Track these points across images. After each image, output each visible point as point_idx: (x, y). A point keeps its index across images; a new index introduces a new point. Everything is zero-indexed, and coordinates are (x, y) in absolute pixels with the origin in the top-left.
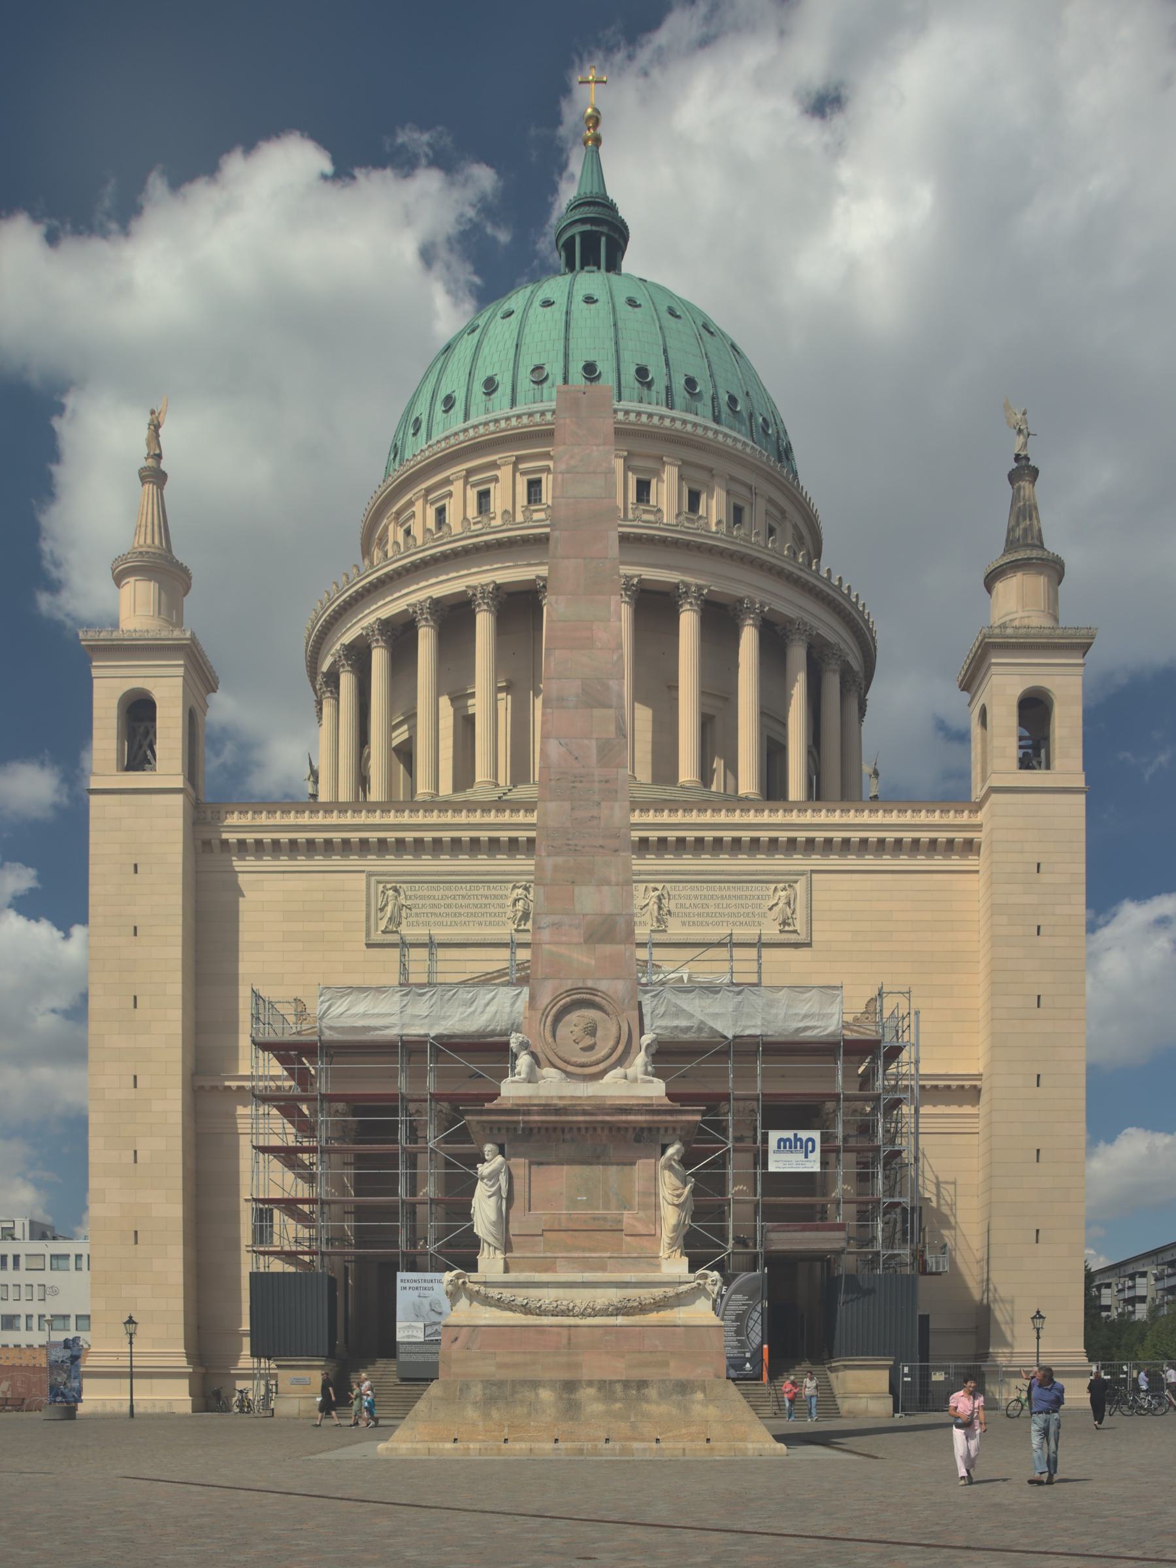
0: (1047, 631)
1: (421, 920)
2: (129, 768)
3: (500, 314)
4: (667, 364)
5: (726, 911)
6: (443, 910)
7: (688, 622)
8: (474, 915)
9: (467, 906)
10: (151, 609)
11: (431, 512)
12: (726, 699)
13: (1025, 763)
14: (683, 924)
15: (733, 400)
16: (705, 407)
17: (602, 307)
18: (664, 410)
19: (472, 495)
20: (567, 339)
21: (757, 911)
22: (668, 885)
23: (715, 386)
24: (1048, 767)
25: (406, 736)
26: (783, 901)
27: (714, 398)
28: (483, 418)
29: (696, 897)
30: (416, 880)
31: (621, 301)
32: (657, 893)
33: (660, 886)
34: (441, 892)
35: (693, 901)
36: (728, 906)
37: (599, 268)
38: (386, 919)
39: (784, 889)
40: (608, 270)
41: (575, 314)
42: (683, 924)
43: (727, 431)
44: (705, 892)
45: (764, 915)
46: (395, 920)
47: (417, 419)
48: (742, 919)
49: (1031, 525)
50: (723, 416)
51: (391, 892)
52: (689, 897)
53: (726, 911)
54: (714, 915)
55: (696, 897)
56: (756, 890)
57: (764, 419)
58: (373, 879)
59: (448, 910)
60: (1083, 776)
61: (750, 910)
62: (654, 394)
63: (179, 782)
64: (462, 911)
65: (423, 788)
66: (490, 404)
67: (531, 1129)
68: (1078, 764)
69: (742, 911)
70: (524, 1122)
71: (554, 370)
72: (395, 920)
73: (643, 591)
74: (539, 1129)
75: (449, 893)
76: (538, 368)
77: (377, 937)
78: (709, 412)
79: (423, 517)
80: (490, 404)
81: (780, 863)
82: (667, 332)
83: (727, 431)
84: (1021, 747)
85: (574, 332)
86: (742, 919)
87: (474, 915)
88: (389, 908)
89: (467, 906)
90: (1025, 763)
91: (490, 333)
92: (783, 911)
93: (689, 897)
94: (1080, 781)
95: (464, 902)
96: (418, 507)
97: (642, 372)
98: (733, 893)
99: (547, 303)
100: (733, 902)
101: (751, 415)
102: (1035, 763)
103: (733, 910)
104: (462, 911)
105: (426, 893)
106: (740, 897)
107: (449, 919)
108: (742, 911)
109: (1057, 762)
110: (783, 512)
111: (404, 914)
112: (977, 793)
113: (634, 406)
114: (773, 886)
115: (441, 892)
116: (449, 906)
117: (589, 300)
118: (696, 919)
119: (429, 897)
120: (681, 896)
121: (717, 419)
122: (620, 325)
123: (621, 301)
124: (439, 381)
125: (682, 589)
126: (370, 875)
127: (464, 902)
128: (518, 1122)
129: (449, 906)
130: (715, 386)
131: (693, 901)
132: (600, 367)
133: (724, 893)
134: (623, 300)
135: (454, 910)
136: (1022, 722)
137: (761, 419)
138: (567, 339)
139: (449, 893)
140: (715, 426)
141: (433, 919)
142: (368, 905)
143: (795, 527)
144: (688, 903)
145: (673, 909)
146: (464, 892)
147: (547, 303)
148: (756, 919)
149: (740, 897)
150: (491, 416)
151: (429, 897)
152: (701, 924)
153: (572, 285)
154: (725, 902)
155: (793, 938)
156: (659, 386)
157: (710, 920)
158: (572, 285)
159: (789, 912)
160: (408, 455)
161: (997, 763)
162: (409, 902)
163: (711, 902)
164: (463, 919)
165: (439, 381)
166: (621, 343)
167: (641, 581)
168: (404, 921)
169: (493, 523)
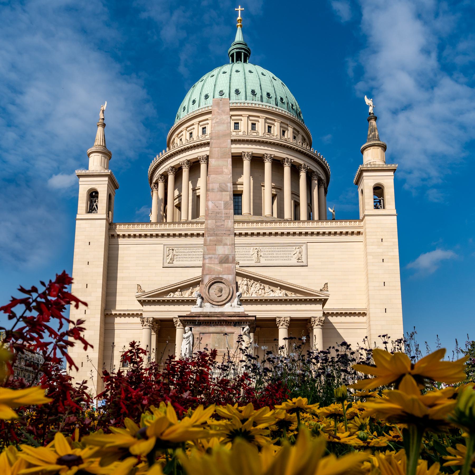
0: (381, 166)
1: (180, 259)
2: (89, 212)
3: (210, 76)
4: (261, 89)
5: (280, 256)
6: (187, 256)
7: (268, 165)
8: (198, 258)
9: (196, 255)
10: (99, 164)
11: (188, 134)
12: (280, 189)
13: (376, 207)
14: (266, 260)
15: (282, 99)
16: (273, 101)
17: (241, 73)
18: (260, 103)
19: (200, 129)
20: (230, 83)
21: (290, 255)
22: (261, 248)
23: (276, 95)
24: (384, 208)
25: (178, 202)
26: (298, 252)
27: (276, 99)
28: (204, 106)
29: (270, 251)
30: (179, 246)
31: (247, 72)
32: (257, 250)
33: (258, 248)
34: (187, 250)
35: (269, 253)
36: (280, 254)
37: (241, 61)
38: (169, 259)
39: (299, 248)
40: (244, 62)
41: (233, 76)
42: (266, 260)
43: (280, 108)
44: (273, 250)
45: (292, 257)
46: (172, 259)
47: (184, 107)
48: (285, 258)
49: (375, 134)
50: (279, 104)
51: (171, 251)
52: (267, 251)
53: (280, 256)
54: (276, 257)
55: (270, 251)
56: (289, 249)
57: (292, 105)
58: (165, 246)
59: (189, 256)
60: (395, 211)
61: (287, 255)
62: (257, 98)
63: (104, 216)
64: (194, 256)
65: (184, 218)
66: (206, 102)
67: (200, 322)
68: (394, 207)
69: (285, 255)
70: (199, 320)
71: (226, 92)
72: (172, 259)
73: (253, 157)
74: (203, 322)
75: (190, 251)
76: (221, 91)
77: (166, 265)
78: (274, 103)
79: (186, 135)
80: (206, 102)
81: (297, 239)
82: (261, 80)
83: (280, 108)
84: (374, 202)
85: (232, 81)
86: (285, 258)
87: (198, 258)
88: (170, 256)
89: (196, 255)
90: (376, 207)
91: (207, 81)
92: (298, 255)
93: (267, 251)
94: (394, 212)
95: (195, 254)
96: (184, 133)
97: (253, 92)
98: (281, 250)
99: (224, 73)
100: (282, 253)
101: (288, 103)
102: (379, 207)
103: (282, 255)
104: (194, 256)
105: (182, 251)
106: (284, 251)
107: (190, 259)
108: (285, 255)
109: (387, 206)
110: (298, 132)
111: (175, 257)
112: (361, 217)
113: (251, 102)
114: (294, 247)
115: (187, 250)
116: (190, 255)
117: (237, 71)
118: (270, 258)
119: (183, 252)
120: (265, 251)
121: (277, 105)
122: (246, 78)
123: (247, 72)
124: (191, 95)
125: (266, 156)
126: (164, 245)
127: (195, 254)
128: (196, 320)
129: (190, 255)
130: (276, 95)
131: (269, 253)
132: (240, 90)
133: (279, 250)
134: (248, 71)
135: (191, 256)
136: (375, 194)
137: (291, 105)
138: (230, 83)
139: (190, 251)
140: (276, 107)
141: (185, 259)
142: (164, 255)
143: (303, 136)
144: (267, 253)
145: (262, 255)
146: (195, 251)
147: (224, 73)
148: (290, 258)
149: (284, 251)
150: (206, 106)
151: (183, 252)
152: (271, 260)
153: (232, 67)
154: (279, 253)
155: (301, 264)
156: (259, 95)
157: (274, 259)
158: (232, 67)
159: (300, 255)
160: (181, 117)
161: (367, 207)
162: (177, 254)
163: (275, 253)
164: (194, 259)
165: (191, 95)
166: (247, 83)
167: (252, 153)
168: (175, 260)
169: (206, 137)
